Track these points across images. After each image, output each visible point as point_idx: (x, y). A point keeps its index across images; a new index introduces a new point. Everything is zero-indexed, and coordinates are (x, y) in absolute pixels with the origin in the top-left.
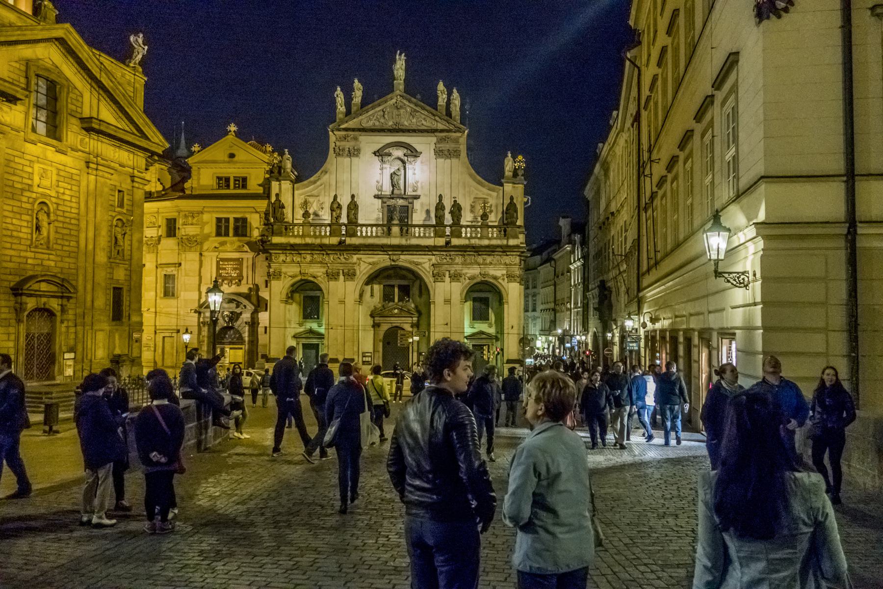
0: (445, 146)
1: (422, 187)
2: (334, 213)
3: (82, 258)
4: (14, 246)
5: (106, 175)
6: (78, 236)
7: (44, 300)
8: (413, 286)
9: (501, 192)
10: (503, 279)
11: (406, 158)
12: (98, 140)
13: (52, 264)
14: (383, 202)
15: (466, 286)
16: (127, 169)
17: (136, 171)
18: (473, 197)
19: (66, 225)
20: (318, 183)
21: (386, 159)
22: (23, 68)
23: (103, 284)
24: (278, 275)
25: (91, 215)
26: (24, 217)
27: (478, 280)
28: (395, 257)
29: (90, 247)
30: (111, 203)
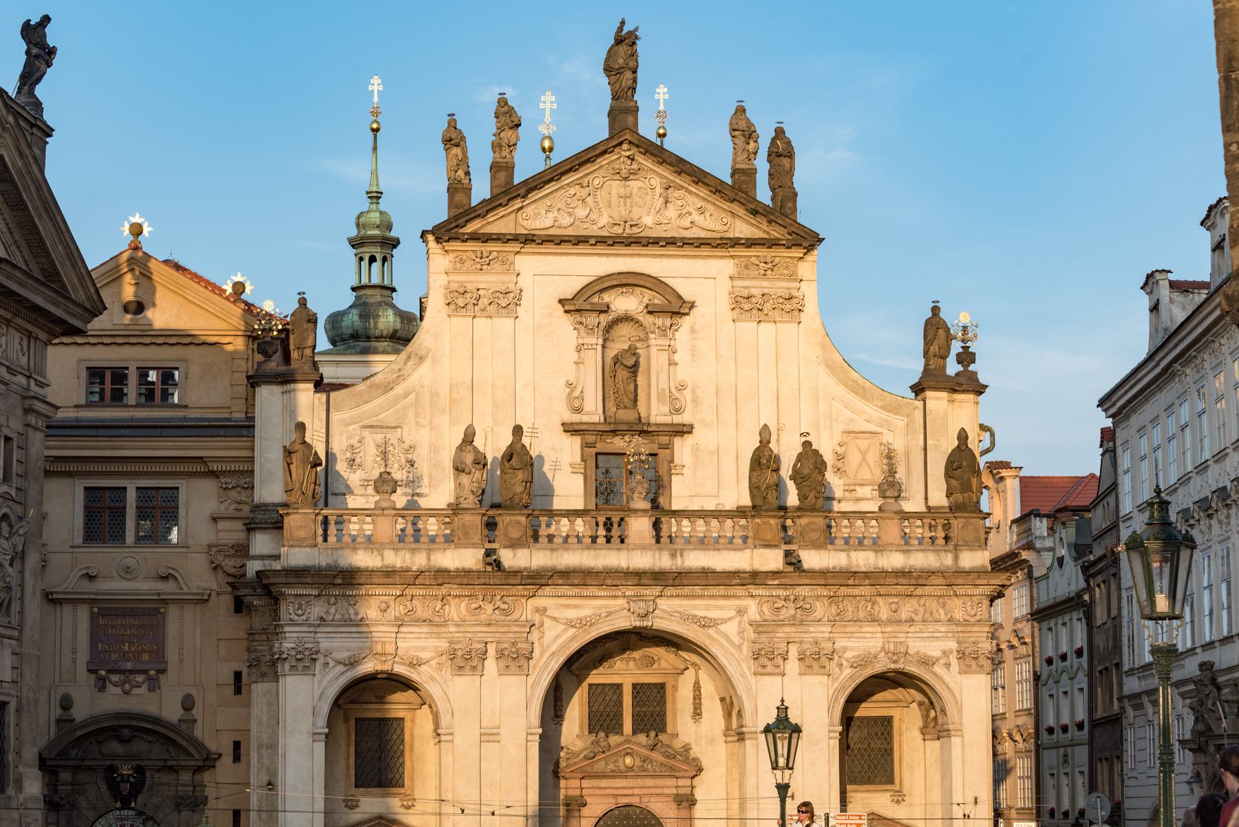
0: (757, 287)
1: (695, 401)
2: (465, 479)
8: (675, 688)
9: (919, 415)
10: (948, 665)
11: (648, 320)
14: (586, 445)
15: (844, 687)
18: (839, 428)
20: (399, 390)
21: (592, 319)
24: (307, 660)
27: (879, 668)
28: (640, 607)
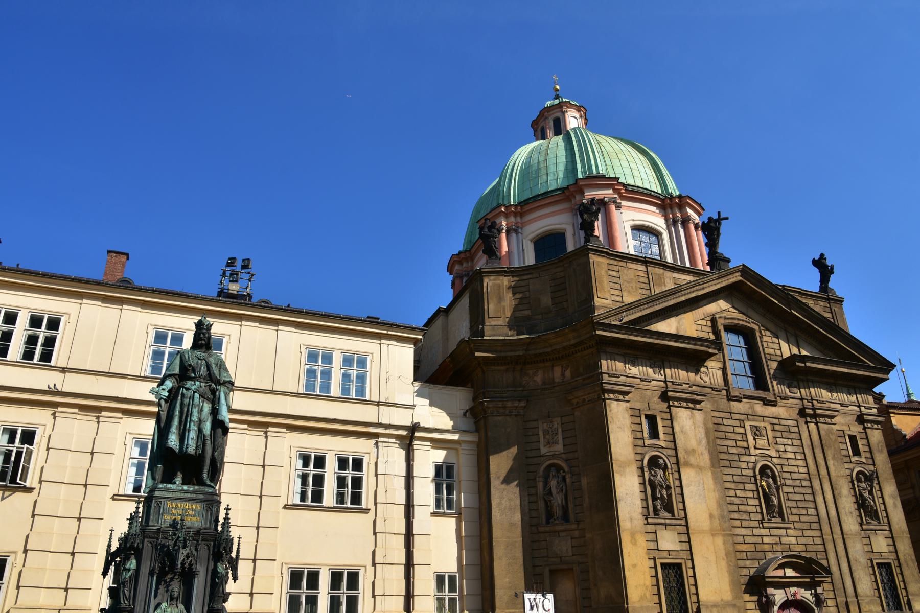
3: (826, 528)
4: (745, 523)
5: (829, 420)
6: (815, 501)
7: (793, 590)
12: (808, 381)
13: (793, 540)
16: (850, 408)
17: (863, 409)
19: (797, 490)
22: (709, 324)
23: (863, 560)
25: (823, 472)
26: (748, 487)
29: (833, 512)
30: (844, 453)
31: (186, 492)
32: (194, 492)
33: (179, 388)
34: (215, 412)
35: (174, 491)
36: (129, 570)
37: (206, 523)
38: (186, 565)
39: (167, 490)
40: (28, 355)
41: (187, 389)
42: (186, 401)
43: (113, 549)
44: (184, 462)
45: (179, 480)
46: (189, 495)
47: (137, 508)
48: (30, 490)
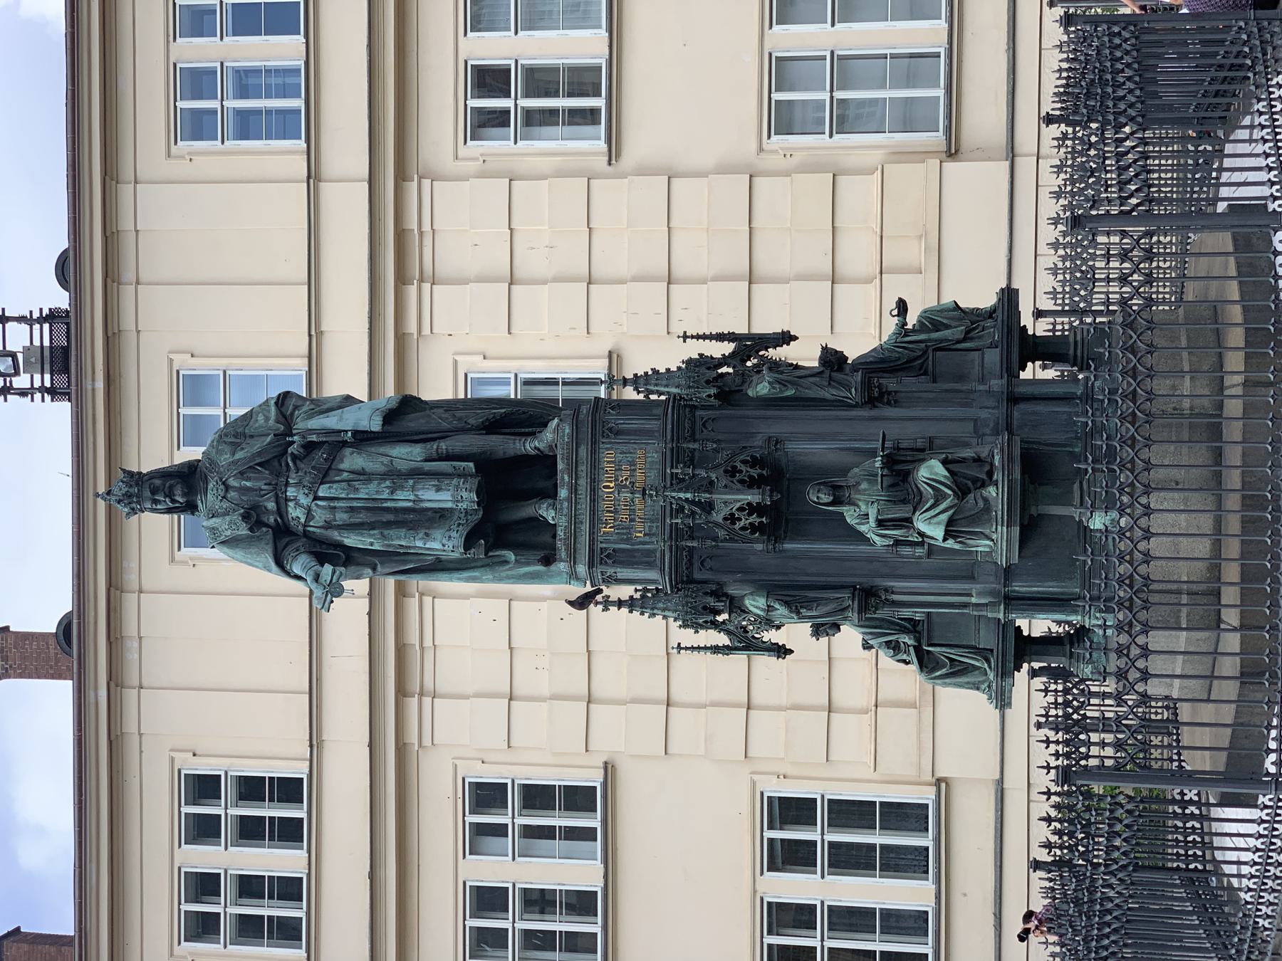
31: (574, 490)
32: (573, 469)
33: (306, 534)
34: (362, 439)
35: (574, 521)
36: (770, 608)
37: (648, 433)
38: (755, 472)
39: (574, 535)
40: (290, 832)
41: (309, 515)
42: (342, 517)
43: (723, 639)
44: (503, 481)
45: (547, 513)
46: (582, 482)
47: (620, 604)
48: (609, 769)
